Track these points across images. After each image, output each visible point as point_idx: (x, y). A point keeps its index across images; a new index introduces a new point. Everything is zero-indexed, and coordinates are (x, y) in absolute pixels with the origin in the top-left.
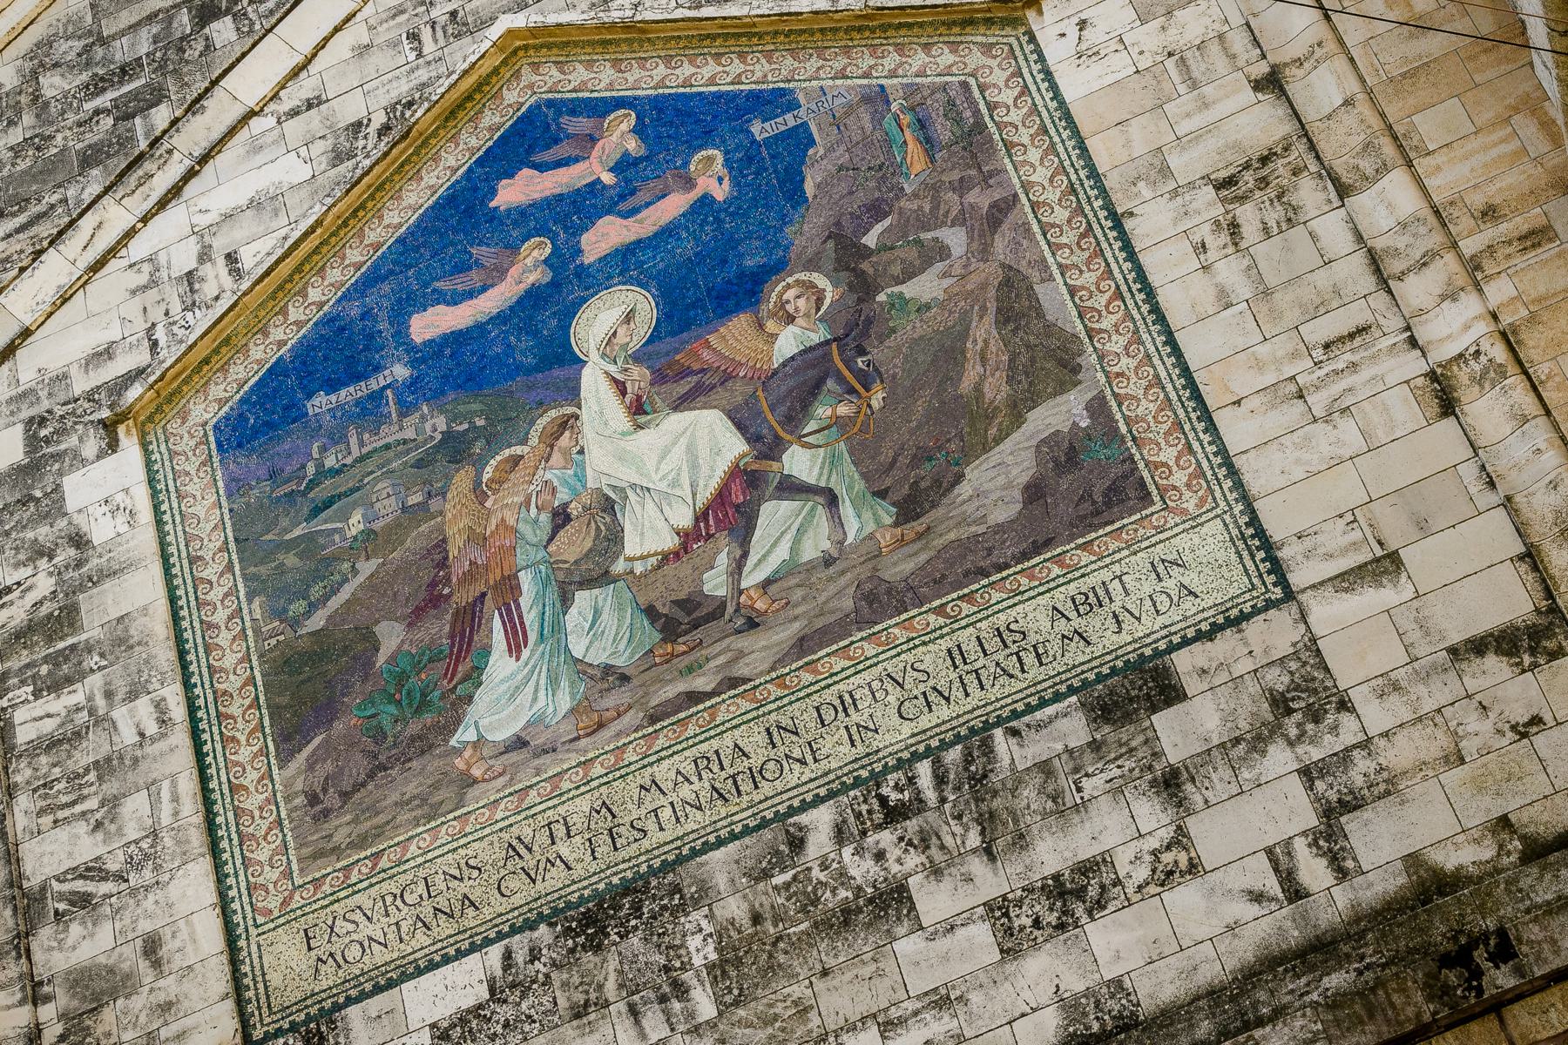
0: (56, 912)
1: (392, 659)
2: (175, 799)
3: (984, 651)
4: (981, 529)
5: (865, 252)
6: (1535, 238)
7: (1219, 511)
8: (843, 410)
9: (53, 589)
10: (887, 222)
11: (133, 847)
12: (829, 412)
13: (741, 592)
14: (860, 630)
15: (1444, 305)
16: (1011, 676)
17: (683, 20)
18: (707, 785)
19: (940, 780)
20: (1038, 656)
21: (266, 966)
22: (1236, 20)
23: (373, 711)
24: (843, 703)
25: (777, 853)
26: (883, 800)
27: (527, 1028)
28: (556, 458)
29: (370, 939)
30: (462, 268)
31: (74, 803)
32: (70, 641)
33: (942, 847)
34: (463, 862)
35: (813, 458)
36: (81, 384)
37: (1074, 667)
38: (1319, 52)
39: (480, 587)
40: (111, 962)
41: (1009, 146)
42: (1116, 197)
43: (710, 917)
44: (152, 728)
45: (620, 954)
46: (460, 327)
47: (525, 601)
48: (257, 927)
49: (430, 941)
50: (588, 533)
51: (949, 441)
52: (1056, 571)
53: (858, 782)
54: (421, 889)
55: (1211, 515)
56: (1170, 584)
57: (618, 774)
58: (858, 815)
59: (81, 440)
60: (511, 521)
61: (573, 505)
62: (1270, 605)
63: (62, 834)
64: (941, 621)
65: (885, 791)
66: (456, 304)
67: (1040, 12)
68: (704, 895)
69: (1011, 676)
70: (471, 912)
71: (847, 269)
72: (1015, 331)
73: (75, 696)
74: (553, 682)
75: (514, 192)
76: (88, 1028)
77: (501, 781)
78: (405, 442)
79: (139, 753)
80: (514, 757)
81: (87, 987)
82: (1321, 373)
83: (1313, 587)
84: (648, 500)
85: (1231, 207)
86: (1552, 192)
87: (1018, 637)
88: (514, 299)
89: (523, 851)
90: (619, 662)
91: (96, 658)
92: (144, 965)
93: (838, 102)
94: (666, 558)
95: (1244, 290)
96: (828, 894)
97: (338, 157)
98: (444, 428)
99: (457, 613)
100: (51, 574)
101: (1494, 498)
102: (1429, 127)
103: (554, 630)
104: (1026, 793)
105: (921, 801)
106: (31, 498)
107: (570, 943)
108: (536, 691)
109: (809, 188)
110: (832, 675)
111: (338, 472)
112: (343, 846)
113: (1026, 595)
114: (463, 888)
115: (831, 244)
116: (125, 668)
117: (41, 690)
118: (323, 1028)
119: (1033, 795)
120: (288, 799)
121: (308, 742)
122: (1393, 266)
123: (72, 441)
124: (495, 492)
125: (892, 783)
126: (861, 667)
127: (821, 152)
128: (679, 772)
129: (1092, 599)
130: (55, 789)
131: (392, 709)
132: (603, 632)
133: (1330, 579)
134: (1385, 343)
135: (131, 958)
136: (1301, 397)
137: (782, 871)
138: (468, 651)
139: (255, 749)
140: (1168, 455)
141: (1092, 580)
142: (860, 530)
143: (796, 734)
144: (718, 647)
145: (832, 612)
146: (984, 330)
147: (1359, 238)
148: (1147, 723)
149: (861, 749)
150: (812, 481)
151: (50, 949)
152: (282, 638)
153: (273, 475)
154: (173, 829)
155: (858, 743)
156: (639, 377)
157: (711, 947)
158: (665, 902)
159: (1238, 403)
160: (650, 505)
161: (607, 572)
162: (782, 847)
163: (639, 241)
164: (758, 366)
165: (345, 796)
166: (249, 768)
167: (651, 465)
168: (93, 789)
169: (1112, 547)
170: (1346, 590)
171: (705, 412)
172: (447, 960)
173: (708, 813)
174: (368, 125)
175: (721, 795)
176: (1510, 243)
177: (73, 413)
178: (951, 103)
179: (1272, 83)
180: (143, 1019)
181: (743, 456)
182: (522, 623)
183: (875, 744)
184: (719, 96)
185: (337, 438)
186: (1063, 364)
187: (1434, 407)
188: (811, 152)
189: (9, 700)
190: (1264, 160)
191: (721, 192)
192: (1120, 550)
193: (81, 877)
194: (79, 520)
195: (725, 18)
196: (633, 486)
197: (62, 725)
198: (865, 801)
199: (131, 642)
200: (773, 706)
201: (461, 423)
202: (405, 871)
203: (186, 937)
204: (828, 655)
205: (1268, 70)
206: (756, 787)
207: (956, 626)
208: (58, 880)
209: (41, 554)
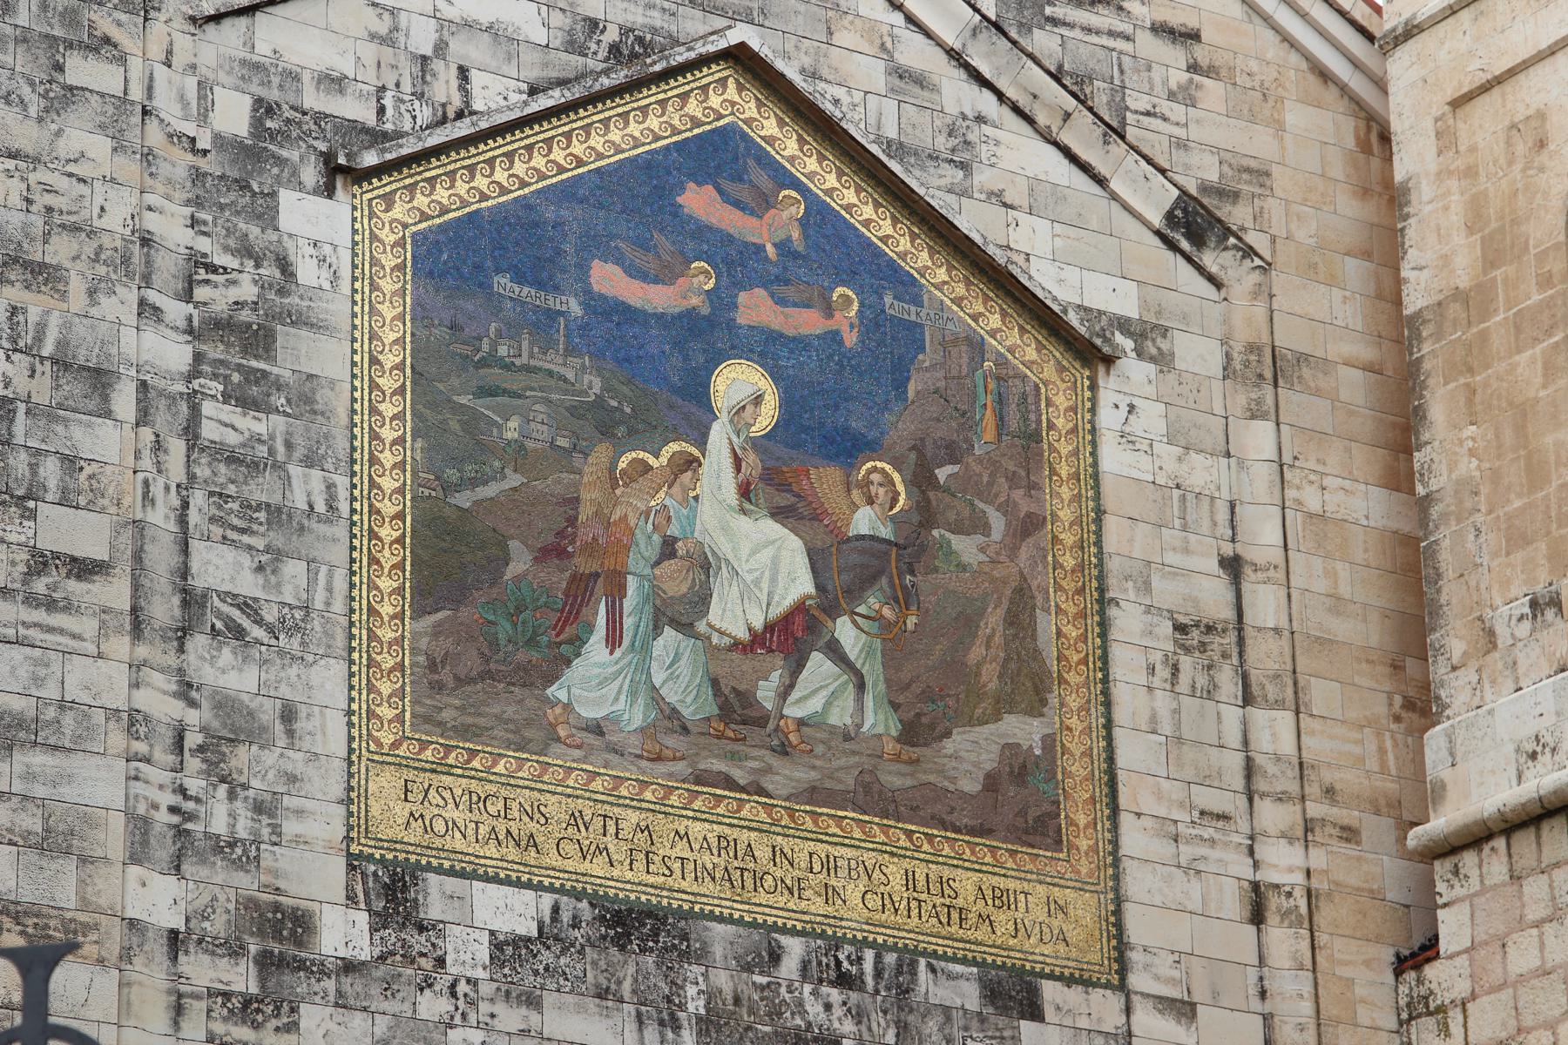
0: (213, 626)
1: (517, 579)
2: (329, 589)
3: (928, 889)
4: (951, 788)
5: (932, 481)
6: (1349, 834)
7: (1098, 888)
8: (887, 612)
9: (255, 299)
10: (956, 468)
11: (286, 610)
12: (877, 606)
13: (782, 717)
14: (854, 811)
15: (1282, 840)
16: (941, 923)
17: (873, 155)
18: (723, 864)
19: (878, 974)
20: (961, 918)
21: (370, 792)
22: (1225, 495)
23: (491, 618)
24: (828, 862)
25: (760, 955)
26: (838, 963)
27: (562, 982)
28: (676, 489)
29: (454, 823)
30: (644, 245)
31: (243, 531)
32: (262, 365)
33: (870, 1029)
34: (536, 804)
35: (857, 637)
36: (313, 100)
37: (980, 944)
38: (1272, 573)
39: (594, 566)
40: (253, 705)
41: (1053, 472)
42: (1112, 581)
43: (706, 976)
44: (320, 507)
45: (637, 964)
46: (632, 303)
47: (629, 603)
48: (369, 751)
49: (497, 856)
50: (686, 579)
51: (949, 696)
52: (988, 859)
53: (823, 935)
54: (500, 805)
55: (1093, 888)
56: (1055, 923)
57: (663, 809)
58: (820, 963)
59: (302, 158)
60: (632, 522)
61: (680, 544)
62: (1107, 986)
63: (229, 554)
64: (908, 844)
65: (841, 957)
66: (630, 276)
67: (1108, 372)
68: (701, 956)
69: (941, 923)
70: (533, 851)
71: (919, 487)
72: (1015, 636)
73: (257, 425)
74: (633, 694)
75: (698, 201)
76: (224, 754)
77: (577, 753)
78: (565, 380)
79: (306, 522)
80: (590, 739)
81: (229, 716)
82: (1194, 832)
83: (1142, 994)
84: (735, 583)
85: (1179, 651)
86: (1368, 806)
87: (952, 894)
88: (677, 310)
89: (583, 829)
90: (686, 712)
91: (283, 401)
92: (279, 728)
93: (950, 326)
94: (736, 645)
95: (1167, 728)
96: (788, 1014)
97: (574, 46)
98: (598, 392)
99: (575, 578)
100: (255, 282)
101: (1256, 1004)
102: (1321, 694)
103: (645, 650)
104: (931, 1024)
105: (863, 982)
106: (248, 187)
107: (603, 929)
108: (619, 692)
109: (911, 394)
110: (827, 834)
111: (508, 367)
112: (449, 725)
113: (967, 864)
114: (533, 826)
115: (913, 456)
116: (308, 430)
117: (230, 397)
118: (407, 879)
119: (935, 1029)
120: (413, 650)
121: (437, 610)
122: (1260, 784)
123: (291, 154)
124: (626, 485)
125: (846, 953)
126: (847, 841)
127: (927, 364)
128: (705, 839)
129: (1005, 898)
130: (230, 505)
131: (508, 627)
132: (678, 676)
133: (1153, 996)
134: (1237, 839)
135: (268, 712)
136: (1176, 841)
137: (761, 973)
138: (576, 618)
139: (395, 585)
140: (1082, 820)
141: (1012, 885)
142: (874, 726)
143: (792, 865)
144: (756, 752)
145: (840, 782)
146: (994, 620)
147: (1246, 742)
148: (1016, 1024)
149: (830, 910)
150: (852, 657)
151: (202, 658)
152: (434, 494)
153: (453, 327)
154: (323, 617)
155: (830, 902)
156: (752, 461)
157: (702, 1003)
158: (676, 942)
159: (1139, 815)
160: (735, 588)
161: (691, 625)
162: (764, 953)
163: (781, 335)
164: (839, 524)
165: (460, 681)
166: (386, 599)
167: (744, 553)
168: (262, 529)
169: (1030, 867)
170: (1160, 1011)
171: (793, 536)
172: (507, 882)
173: (718, 888)
174: (602, 32)
175: (730, 880)
176: (1335, 825)
177: (299, 124)
178: (1024, 396)
179: (1233, 566)
180: (271, 775)
181: (809, 597)
182: (621, 624)
183: (842, 912)
184: (870, 244)
185: (511, 331)
186: (1036, 687)
187: (1247, 914)
188: (920, 357)
189: (200, 385)
190: (1210, 629)
191: (851, 339)
192: (1032, 873)
193: (238, 606)
194: (289, 244)
195: (903, 182)
196: (727, 561)
197: (244, 445)
198: (826, 955)
199: (318, 407)
200: (779, 829)
201: (612, 398)
202: (491, 781)
203: (318, 724)
204: (827, 815)
205: (1232, 554)
206: (755, 890)
207: (916, 855)
208: (219, 596)
209: (250, 256)
